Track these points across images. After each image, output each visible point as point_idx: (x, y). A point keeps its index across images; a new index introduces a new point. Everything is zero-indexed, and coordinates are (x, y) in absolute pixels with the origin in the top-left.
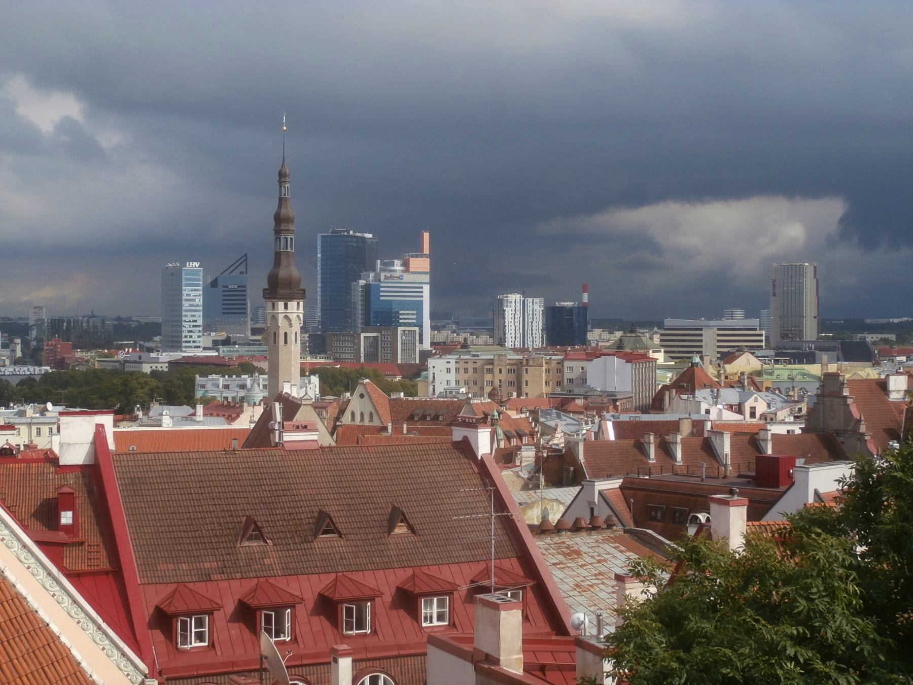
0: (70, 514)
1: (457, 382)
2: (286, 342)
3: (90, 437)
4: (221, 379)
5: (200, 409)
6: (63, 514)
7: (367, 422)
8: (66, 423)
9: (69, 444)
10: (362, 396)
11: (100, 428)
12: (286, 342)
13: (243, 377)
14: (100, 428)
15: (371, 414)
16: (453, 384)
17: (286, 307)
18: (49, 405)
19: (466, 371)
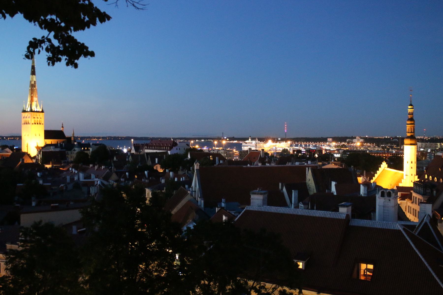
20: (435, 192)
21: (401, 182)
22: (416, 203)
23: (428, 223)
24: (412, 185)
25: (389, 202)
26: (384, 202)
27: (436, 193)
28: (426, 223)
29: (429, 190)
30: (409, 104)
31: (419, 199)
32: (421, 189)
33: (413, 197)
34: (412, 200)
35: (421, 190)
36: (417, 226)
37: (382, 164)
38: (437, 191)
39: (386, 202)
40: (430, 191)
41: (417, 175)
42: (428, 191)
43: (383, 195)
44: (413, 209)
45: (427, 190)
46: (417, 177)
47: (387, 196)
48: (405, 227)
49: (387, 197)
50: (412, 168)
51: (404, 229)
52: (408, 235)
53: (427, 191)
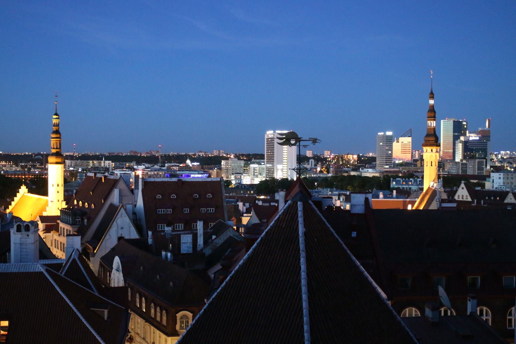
0: (355, 233)
1: (504, 183)
2: (432, 166)
3: (363, 203)
4: (401, 180)
5: (395, 192)
6: (353, 232)
7: (465, 200)
8: (354, 197)
9: (355, 205)
10: (463, 188)
11: (367, 200)
12: (432, 166)
13: (411, 179)
14: (367, 200)
15: (467, 196)
16: (502, 184)
17: (432, 151)
18: (335, 189)
19: (508, 178)
20: (86, 220)
21: (45, 211)
22: (64, 236)
23: (77, 259)
24: (58, 213)
25: (27, 238)
26: (21, 238)
27: (88, 222)
28: (74, 260)
29: (79, 218)
30: (54, 113)
31: (67, 230)
32: (70, 218)
33: (61, 228)
34: (59, 232)
35: (70, 219)
36: (63, 265)
37: (20, 188)
38: (89, 219)
39: (23, 238)
40: (80, 220)
41: (64, 201)
42: (78, 220)
43: (19, 230)
44: (61, 243)
45: (77, 219)
46: (65, 202)
47: (25, 231)
48: (48, 268)
49: (24, 231)
50: (58, 192)
51: (47, 270)
52: (52, 278)
53: (76, 220)
